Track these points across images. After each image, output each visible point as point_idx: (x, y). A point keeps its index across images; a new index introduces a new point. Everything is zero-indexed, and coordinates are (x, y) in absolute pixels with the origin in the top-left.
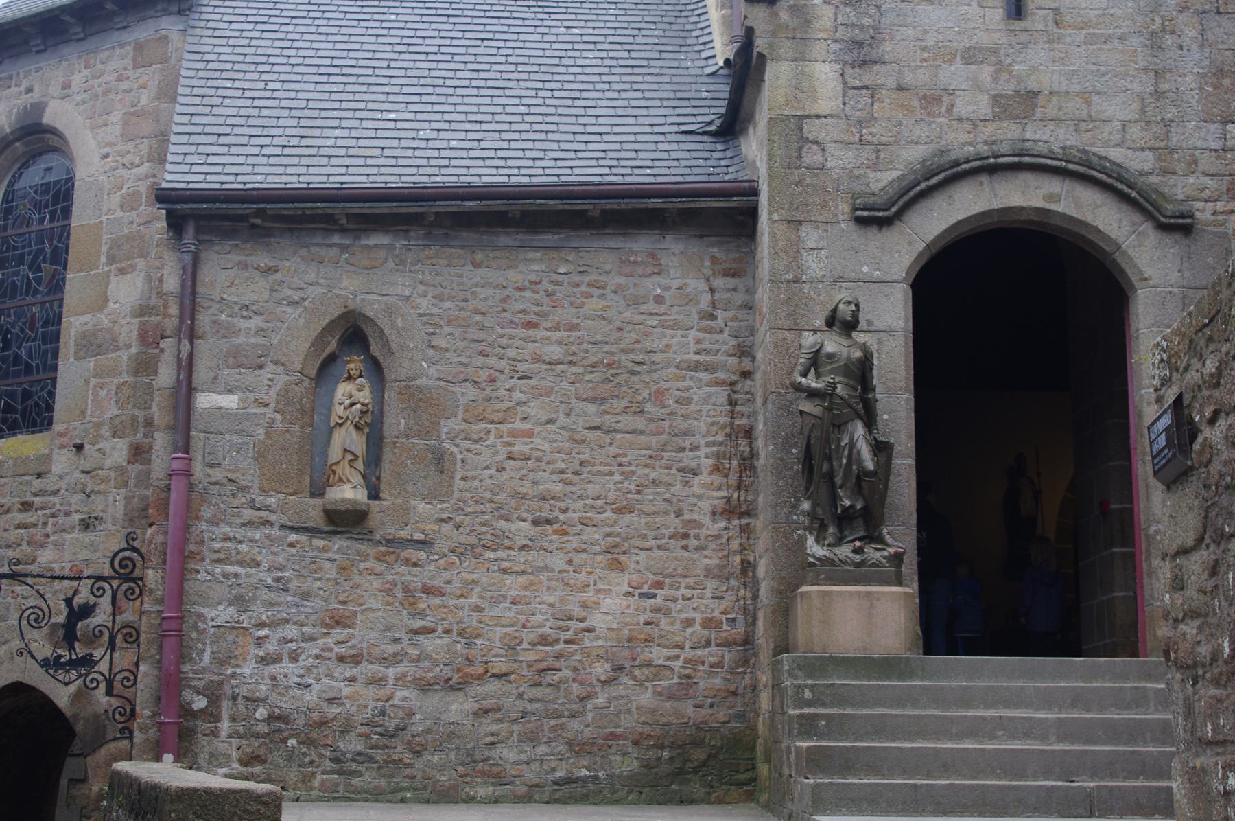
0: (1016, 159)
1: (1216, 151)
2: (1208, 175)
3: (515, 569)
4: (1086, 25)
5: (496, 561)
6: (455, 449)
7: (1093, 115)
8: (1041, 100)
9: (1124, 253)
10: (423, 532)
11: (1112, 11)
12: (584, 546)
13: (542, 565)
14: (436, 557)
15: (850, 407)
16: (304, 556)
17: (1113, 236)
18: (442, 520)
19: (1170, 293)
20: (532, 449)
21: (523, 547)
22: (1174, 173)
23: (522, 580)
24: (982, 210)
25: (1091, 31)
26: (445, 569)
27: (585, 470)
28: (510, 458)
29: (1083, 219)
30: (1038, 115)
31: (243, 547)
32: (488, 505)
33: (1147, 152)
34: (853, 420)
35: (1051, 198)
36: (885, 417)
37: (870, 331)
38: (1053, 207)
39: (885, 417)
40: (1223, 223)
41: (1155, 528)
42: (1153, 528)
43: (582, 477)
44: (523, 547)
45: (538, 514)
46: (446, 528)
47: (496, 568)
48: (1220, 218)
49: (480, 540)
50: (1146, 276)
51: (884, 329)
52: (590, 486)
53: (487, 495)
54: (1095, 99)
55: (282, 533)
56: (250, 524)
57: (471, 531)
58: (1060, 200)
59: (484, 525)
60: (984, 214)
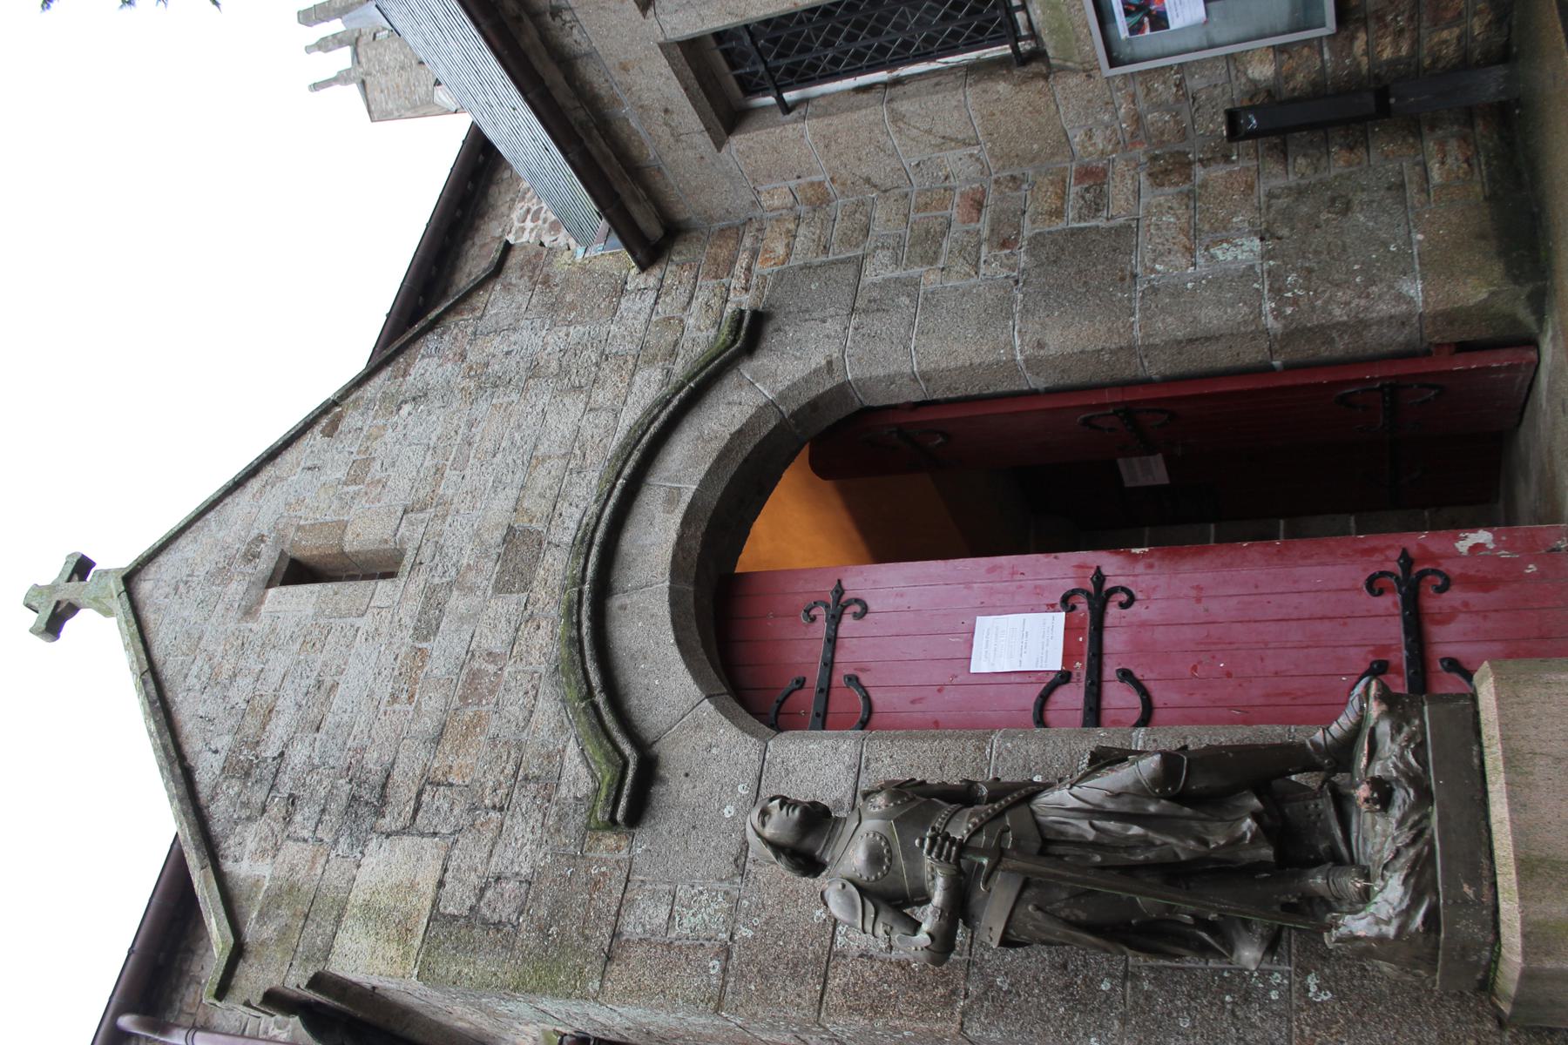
0: (595, 550)
1: (658, 297)
2: (689, 303)
4: (439, 471)
7: (563, 451)
8: (522, 522)
9: (783, 396)
11: (434, 439)
17: (751, 411)
19: (856, 329)
22: (676, 343)
24: (667, 605)
25: (449, 463)
29: (715, 455)
30: (537, 526)
33: (637, 378)
35: (671, 500)
38: (687, 498)
40: (765, 278)
41: (1270, 318)
42: (1270, 322)
48: (754, 281)
50: (824, 362)
54: (542, 449)
58: (679, 488)
60: (674, 603)
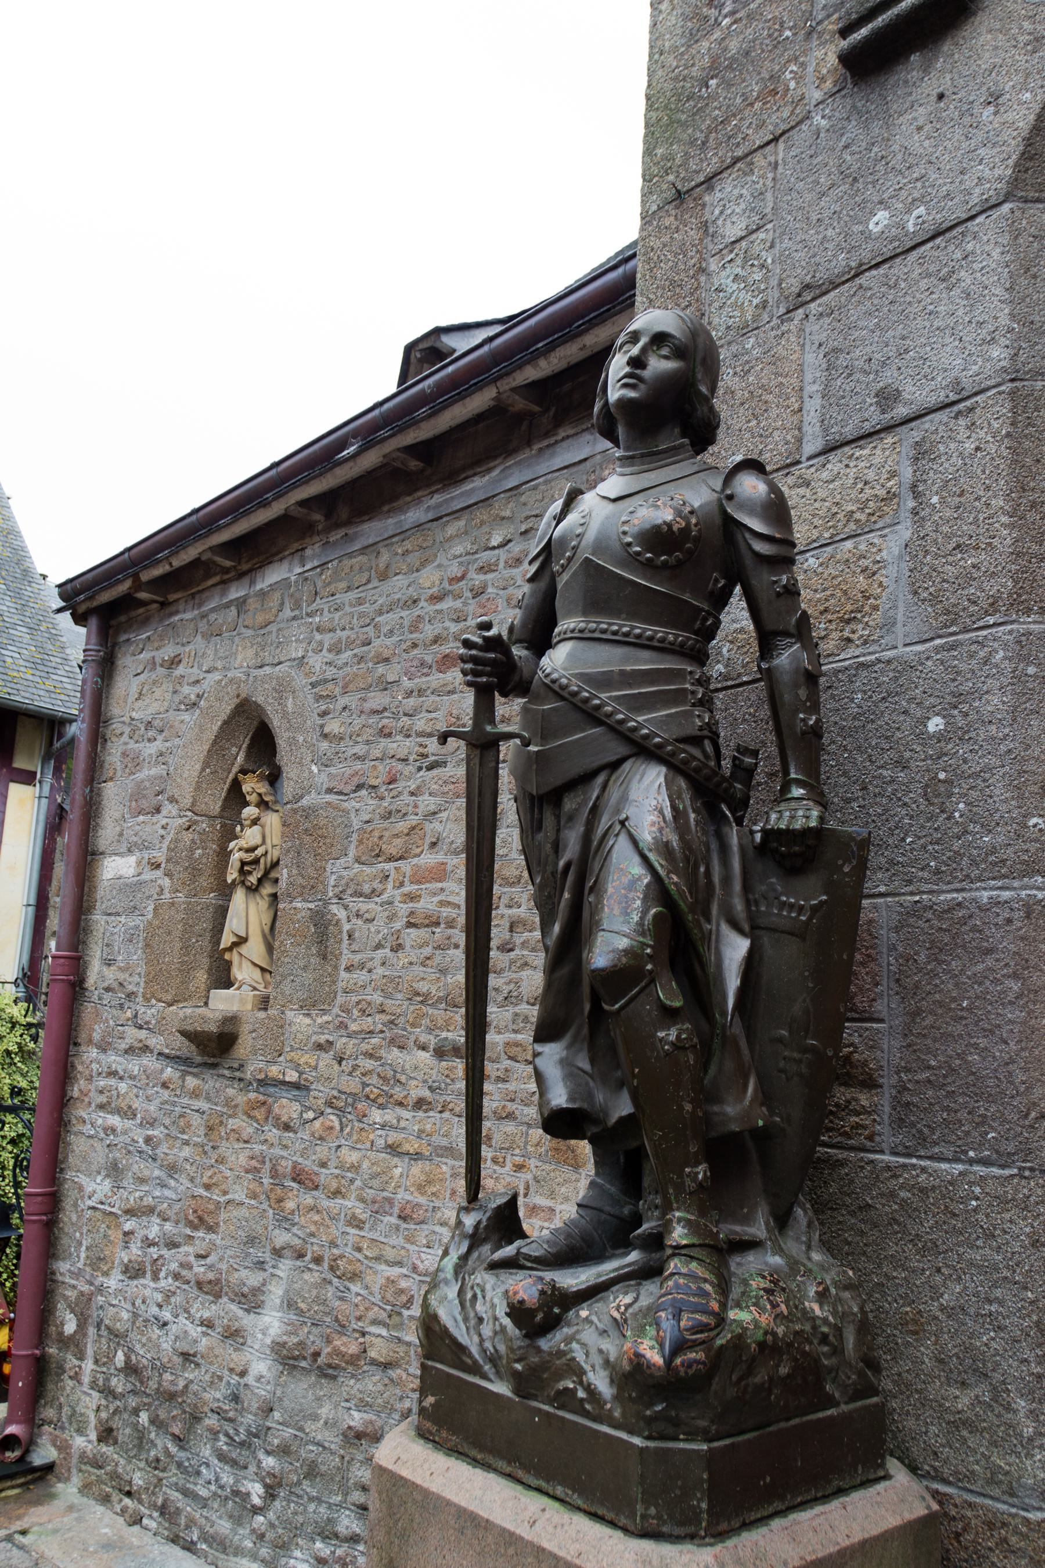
3: (406, 1147)
5: (383, 1126)
6: (342, 914)
10: (297, 1067)
12: (511, 1106)
13: (444, 1142)
14: (310, 1115)
15: (592, 716)
16: (174, 1104)
18: (319, 1047)
20: (442, 903)
21: (420, 1104)
23: (417, 1170)
26: (321, 1138)
27: (519, 939)
28: (410, 925)
31: (123, 1087)
32: (378, 1017)
34: (615, 766)
36: (935, 724)
37: (888, 429)
39: (935, 724)
43: (512, 954)
44: (420, 1104)
45: (444, 1034)
46: (326, 1059)
47: (380, 1143)
49: (365, 1085)
51: (932, 400)
52: (525, 974)
53: (377, 998)
55: (158, 1066)
56: (130, 1051)
57: (355, 1067)
59: (371, 1056)
